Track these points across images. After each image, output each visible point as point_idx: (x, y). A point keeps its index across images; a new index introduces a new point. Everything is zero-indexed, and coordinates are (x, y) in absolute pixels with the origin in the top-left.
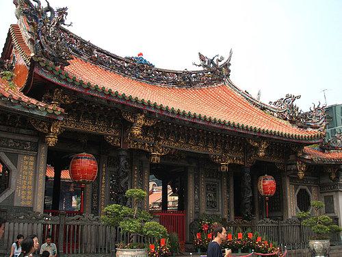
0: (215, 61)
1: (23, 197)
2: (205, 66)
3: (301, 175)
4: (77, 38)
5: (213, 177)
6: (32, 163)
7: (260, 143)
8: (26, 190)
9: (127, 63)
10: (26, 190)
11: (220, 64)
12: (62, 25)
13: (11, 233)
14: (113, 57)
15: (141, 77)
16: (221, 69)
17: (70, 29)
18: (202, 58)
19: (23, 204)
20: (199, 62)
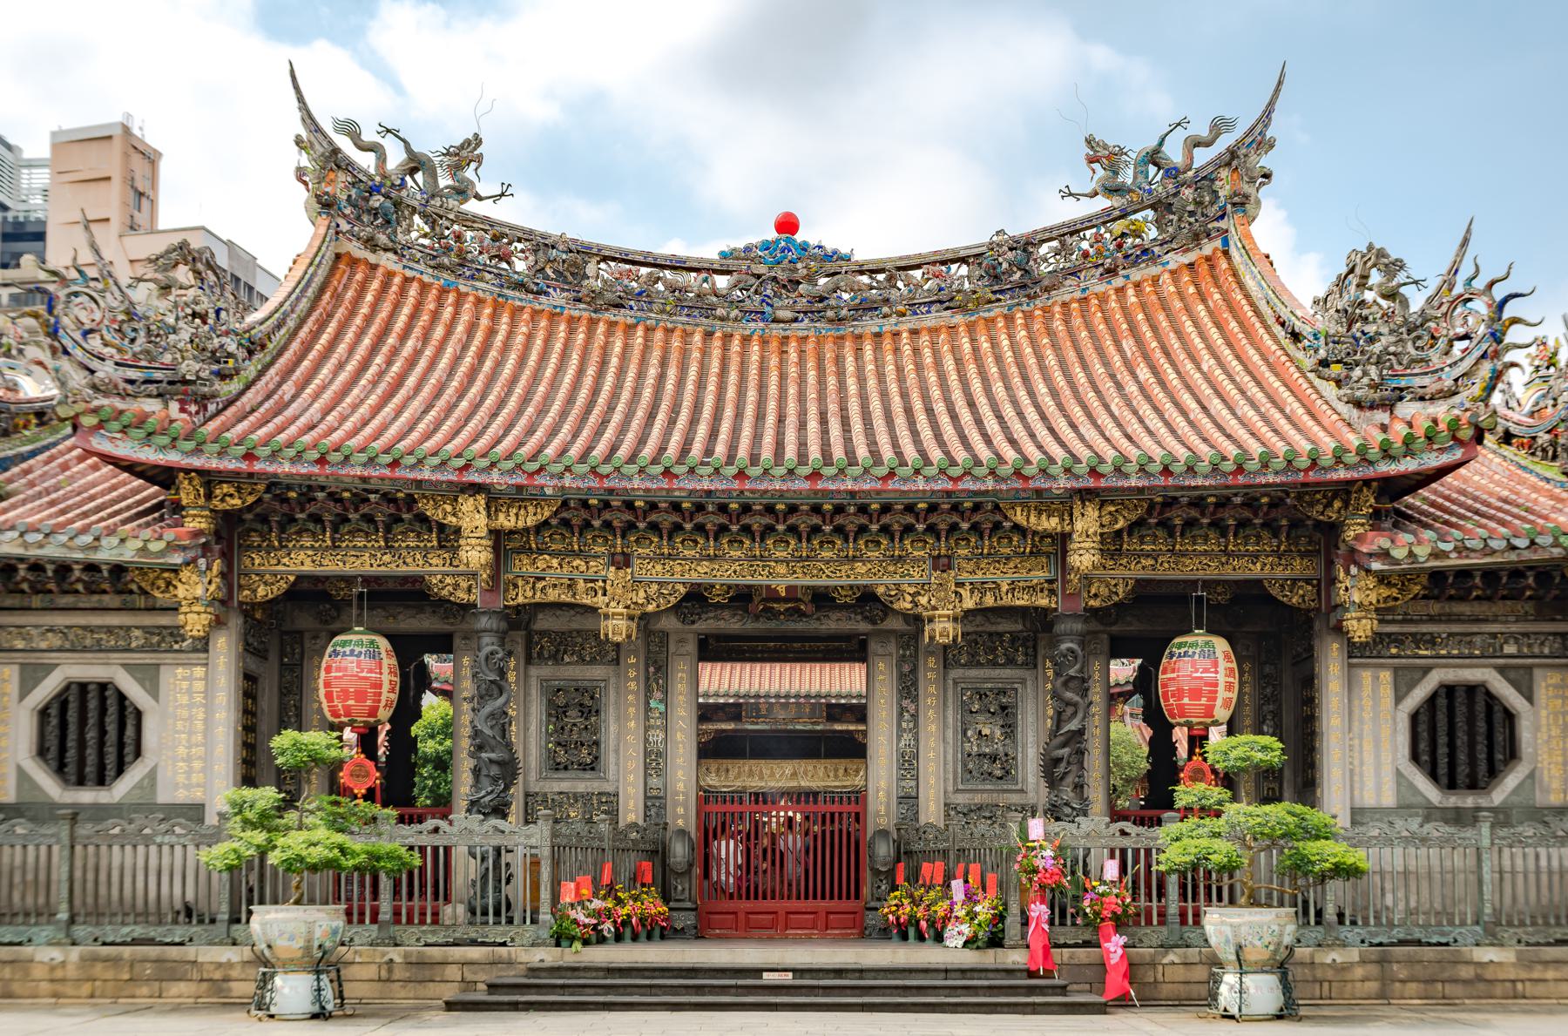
0: (1174, 153)
1: (181, 779)
2: (1113, 190)
3: (1360, 628)
4: (526, 236)
5: (994, 664)
6: (199, 686)
7: (1067, 512)
8: (188, 759)
9: (728, 272)
10: (188, 759)
11: (1202, 157)
12: (472, 206)
13: (103, 877)
14: (663, 267)
15: (788, 314)
16: (1205, 181)
17: (501, 212)
18: (1102, 155)
19: (182, 796)
20: (1088, 178)
